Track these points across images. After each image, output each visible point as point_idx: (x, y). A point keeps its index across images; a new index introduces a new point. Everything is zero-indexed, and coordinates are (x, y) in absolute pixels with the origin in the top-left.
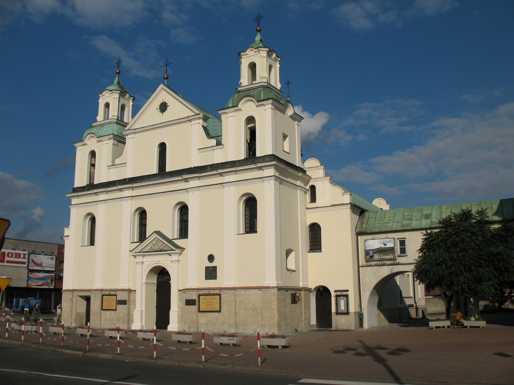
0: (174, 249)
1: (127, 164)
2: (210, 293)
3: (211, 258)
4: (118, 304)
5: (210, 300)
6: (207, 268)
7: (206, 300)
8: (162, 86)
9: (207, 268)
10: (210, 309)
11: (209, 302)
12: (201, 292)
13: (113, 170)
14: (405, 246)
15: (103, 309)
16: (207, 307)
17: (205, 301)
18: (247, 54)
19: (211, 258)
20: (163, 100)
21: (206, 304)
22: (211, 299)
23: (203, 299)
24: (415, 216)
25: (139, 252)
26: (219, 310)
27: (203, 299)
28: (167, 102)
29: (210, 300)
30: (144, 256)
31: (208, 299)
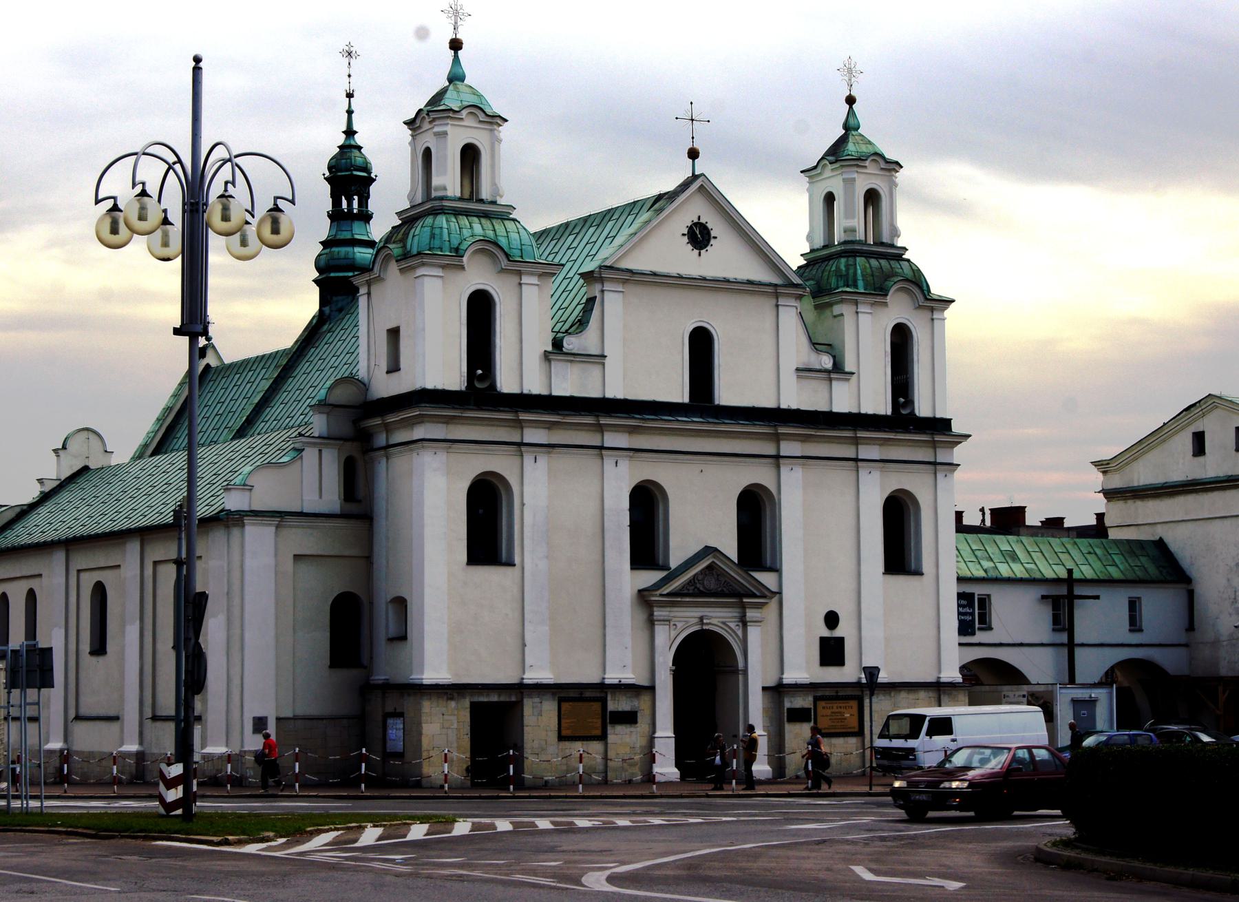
0: (758, 594)
1: (607, 361)
2: (839, 694)
3: (832, 619)
4: (610, 723)
5: (839, 710)
6: (824, 641)
7: (832, 710)
8: (703, 181)
9: (824, 641)
10: (838, 728)
11: (837, 713)
12: (819, 694)
13: (558, 367)
14: (985, 609)
15: (561, 738)
16: (833, 724)
17: (829, 712)
18: (865, 167)
19: (832, 619)
20: (699, 217)
21: (831, 717)
22: (841, 707)
23: (824, 708)
24: (993, 554)
25: (668, 595)
26: (856, 730)
27: (824, 708)
28: (710, 227)
29: (839, 710)
30: (673, 604)
31: (835, 707)
